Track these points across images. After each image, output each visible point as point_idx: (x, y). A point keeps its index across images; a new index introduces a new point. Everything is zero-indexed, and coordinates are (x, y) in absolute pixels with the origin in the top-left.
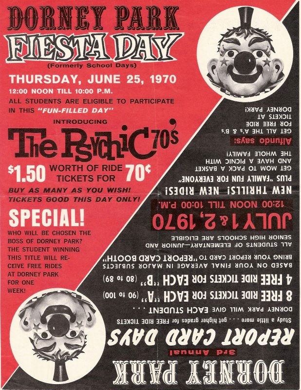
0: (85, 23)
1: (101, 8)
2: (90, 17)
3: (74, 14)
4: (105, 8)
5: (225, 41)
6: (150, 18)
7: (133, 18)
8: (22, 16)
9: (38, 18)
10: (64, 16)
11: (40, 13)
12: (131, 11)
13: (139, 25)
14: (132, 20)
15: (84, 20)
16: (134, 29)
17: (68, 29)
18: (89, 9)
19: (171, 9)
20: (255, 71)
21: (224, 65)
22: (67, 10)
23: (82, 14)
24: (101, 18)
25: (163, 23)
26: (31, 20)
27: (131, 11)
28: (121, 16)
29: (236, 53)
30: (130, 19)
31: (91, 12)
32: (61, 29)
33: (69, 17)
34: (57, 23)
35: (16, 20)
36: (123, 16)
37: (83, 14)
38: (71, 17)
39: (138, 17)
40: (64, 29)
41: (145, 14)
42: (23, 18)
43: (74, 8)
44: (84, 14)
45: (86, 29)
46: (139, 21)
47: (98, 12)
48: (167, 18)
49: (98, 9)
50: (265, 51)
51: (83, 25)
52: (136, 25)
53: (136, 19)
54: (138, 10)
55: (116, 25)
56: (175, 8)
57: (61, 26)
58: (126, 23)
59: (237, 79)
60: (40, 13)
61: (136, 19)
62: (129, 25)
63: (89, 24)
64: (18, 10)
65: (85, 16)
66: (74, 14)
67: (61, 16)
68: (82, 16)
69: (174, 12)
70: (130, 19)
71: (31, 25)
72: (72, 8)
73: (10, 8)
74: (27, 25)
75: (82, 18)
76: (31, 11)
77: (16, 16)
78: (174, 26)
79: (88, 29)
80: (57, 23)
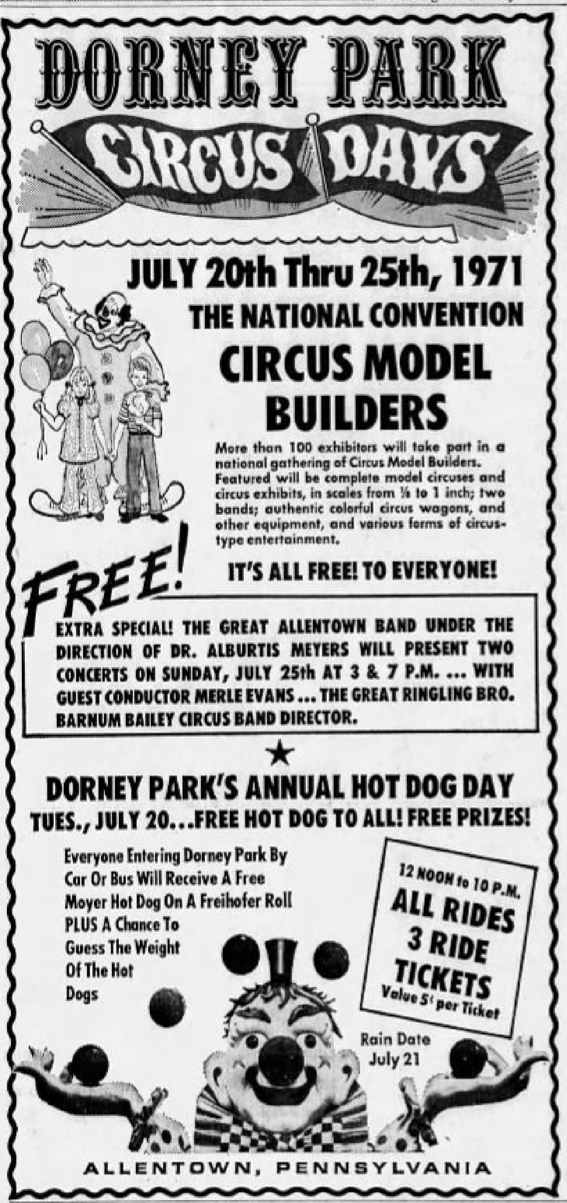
0: (250, 86)
1: (294, 42)
2: (263, 71)
3: (218, 57)
4: (304, 43)
5: (241, 1014)
6: (423, 70)
7: (377, 71)
8: (77, 66)
9: (119, 73)
10: (190, 66)
11: (125, 59)
12: (373, 52)
14: (376, 79)
15: (244, 79)
17: (200, 105)
18: (260, 47)
19: (482, 45)
20: (301, 1080)
21: (239, 1067)
22: (197, 50)
23: (239, 61)
24: (291, 72)
25: (461, 89)
26: (102, 80)
27: (373, 52)
28: (348, 65)
29: (262, 1040)
30: (369, 76)
31: (265, 53)
32: (180, 105)
33: (202, 68)
34: (170, 90)
35: (61, 79)
37: (244, 60)
38: (210, 71)
39: (392, 70)
40: (190, 105)
41: (410, 58)
43: (216, 43)
44: (244, 60)
45: (248, 105)
46: (396, 81)
47: (285, 54)
48: (472, 72)
49: (284, 45)
50: (321, 1035)
51: (243, 93)
52: (386, 93)
53: (387, 75)
54: (391, 48)
55: (332, 91)
57: (180, 96)
58: (360, 89)
59: (264, 1096)
60: (125, 59)
61: (387, 75)
63: (258, 89)
65: (248, 66)
66: (218, 57)
67: (179, 71)
68: (241, 67)
71: (101, 93)
72: (212, 45)
75: (239, 74)
76: (102, 53)
77: (61, 64)
78: (490, 95)
79: (256, 105)
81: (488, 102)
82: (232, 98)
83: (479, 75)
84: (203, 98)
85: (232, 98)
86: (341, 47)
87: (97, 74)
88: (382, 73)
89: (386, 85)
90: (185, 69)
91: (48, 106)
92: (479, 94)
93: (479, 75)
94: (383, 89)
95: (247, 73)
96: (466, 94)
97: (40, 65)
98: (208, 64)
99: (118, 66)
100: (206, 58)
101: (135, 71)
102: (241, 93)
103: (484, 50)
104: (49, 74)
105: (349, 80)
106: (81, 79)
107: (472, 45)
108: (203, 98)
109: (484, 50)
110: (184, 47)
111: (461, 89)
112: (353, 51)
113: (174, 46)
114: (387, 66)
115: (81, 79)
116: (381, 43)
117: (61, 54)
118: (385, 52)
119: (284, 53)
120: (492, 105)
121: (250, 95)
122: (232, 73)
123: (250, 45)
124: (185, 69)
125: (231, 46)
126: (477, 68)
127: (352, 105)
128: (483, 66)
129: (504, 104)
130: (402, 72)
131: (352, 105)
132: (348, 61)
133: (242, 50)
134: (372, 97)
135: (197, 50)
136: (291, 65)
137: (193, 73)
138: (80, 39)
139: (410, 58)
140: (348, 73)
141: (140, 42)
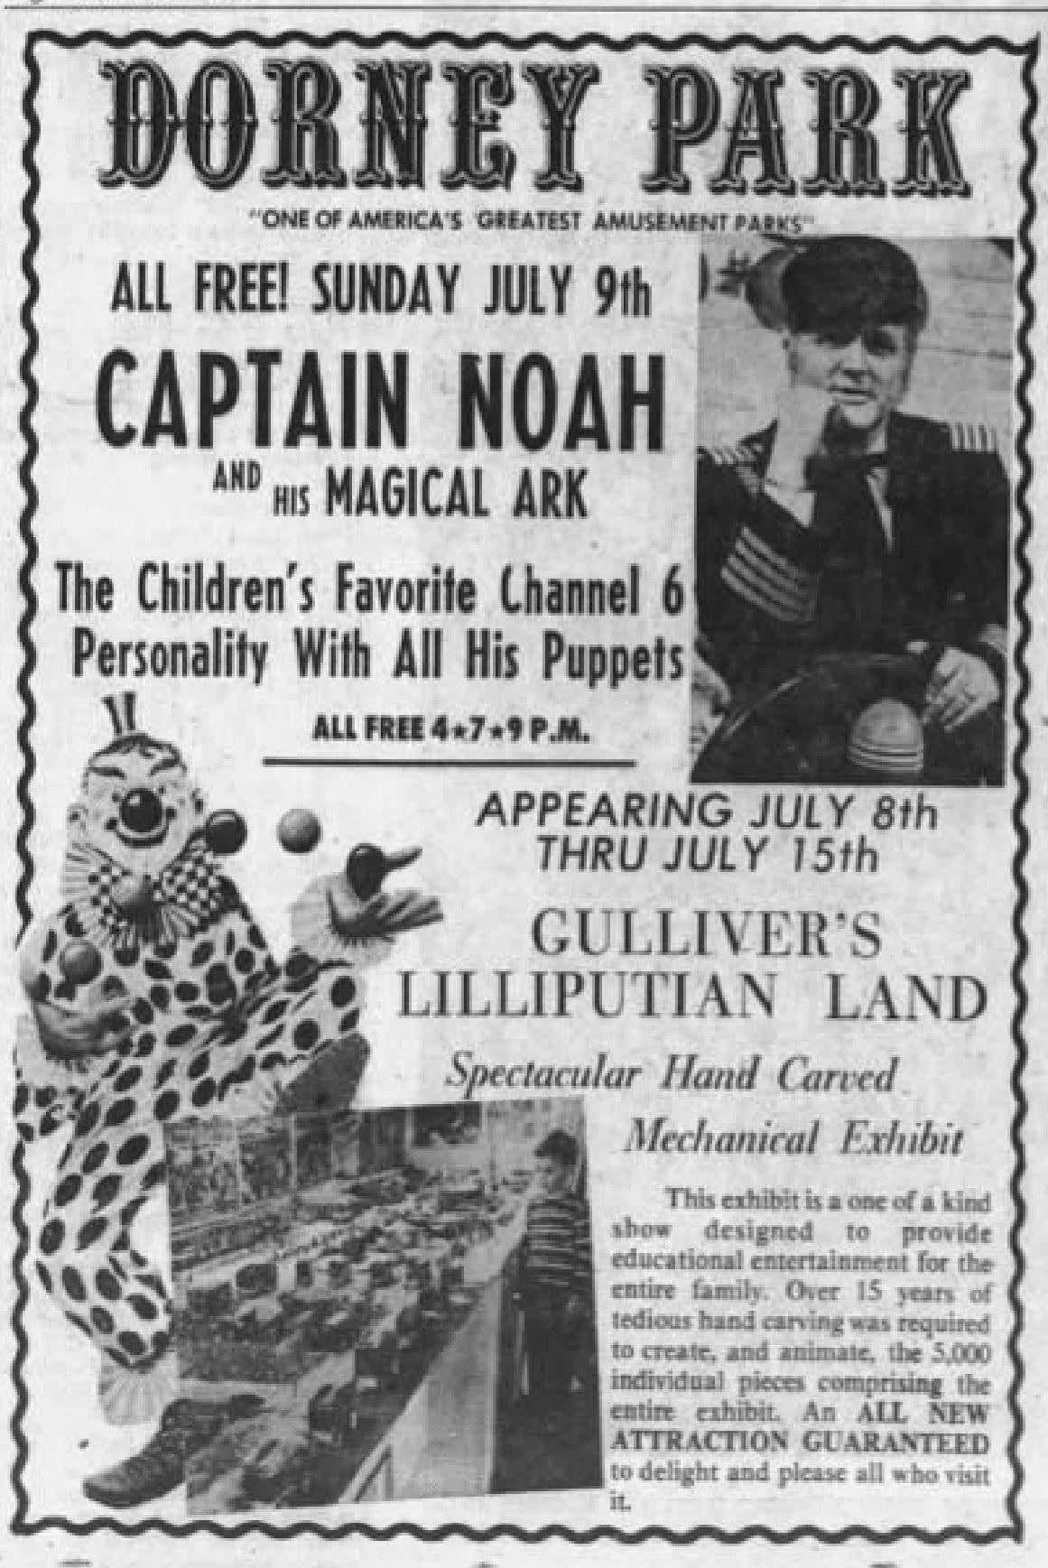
0: (496, 152)
2: (521, 127)
3: (439, 100)
6: (822, 127)
7: (736, 128)
8: (173, 109)
9: (254, 125)
11: (266, 96)
12: (729, 96)
13: (769, 171)
14: (734, 142)
15: (487, 138)
16: (742, 190)
17: (404, 183)
18: (517, 80)
19: (933, 83)
22: (401, 86)
24: (572, 128)
25: (892, 162)
27: (729, 96)
28: (679, 117)
30: (720, 139)
31: (525, 91)
33: (409, 120)
34: (352, 154)
35: (144, 133)
36: (688, 116)
37: (486, 105)
38: (423, 124)
39: (764, 127)
41: (797, 109)
42: (176, 125)
44: (486, 105)
46: (771, 145)
47: (562, 95)
49: (562, 78)
51: (485, 164)
52: (752, 168)
54: (761, 89)
55: (648, 166)
56: (949, 80)
57: (370, 166)
60: (266, 96)
61: (754, 135)
62: (716, 166)
63: (512, 158)
64: (154, 76)
65: (495, 117)
66: (439, 100)
67: (369, 121)
68: (481, 117)
69: (949, 100)
70: (720, 139)
71: (218, 160)
72: (427, 77)
73: (116, 70)
74: (198, 166)
75: (481, 128)
76: (220, 90)
77: (144, 106)
78: (944, 175)
79: (507, 186)
80: (352, 154)
81: (941, 186)
82: (462, 173)
83: (926, 139)
84: (412, 173)
85: (462, 173)
86: (666, 85)
87: (210, 125)
88: (746, 132)
89: (753, 154)
90: (379, 118)
91: (119, 182)
92: (925, 173)
93: (926, 139)
94: (746, 160)
95: (494, 128)
96: (901, 173)
97: (107, 108)
98: (421, 109)
99: (252, 111)
100: (416, 101)
101: (284, 120)
102: (481, 164)
103: (934, 95)
104: (122, 125)
105: (679, 144)
106: (181, 135)
107: (914, 85)
108: (412, 173)
109: (934, 95)
110: (376, 78)
111: (892, 162)
112: (688, 93)
113: (359, 77)
114: (755, 122)
115: (181, 135)
116: (744, 77)
117: (144, 89)
118: (750, 94)
119: (560, 93)
120: (946, 192)
121: (497, 169)
122: (466, 127)
123: (498, 76)
124: (379, 118)
125: (463, 79)
126: (922, 126)
127: (685, 188)
128: (932, 121)
129: (966, 192)
130: (780, 131)
131: (685, 188)
132: (680, 108)
133: (484, 87)
134: (726, 173)
135: (401, 86)
136: (572, 117)
137: (394, 126)
138: (182, 66)
139: (797, 109)
140: (678, 131)
141: (295, 69)
